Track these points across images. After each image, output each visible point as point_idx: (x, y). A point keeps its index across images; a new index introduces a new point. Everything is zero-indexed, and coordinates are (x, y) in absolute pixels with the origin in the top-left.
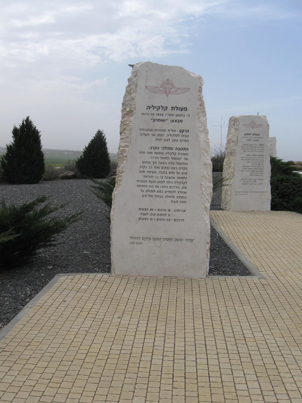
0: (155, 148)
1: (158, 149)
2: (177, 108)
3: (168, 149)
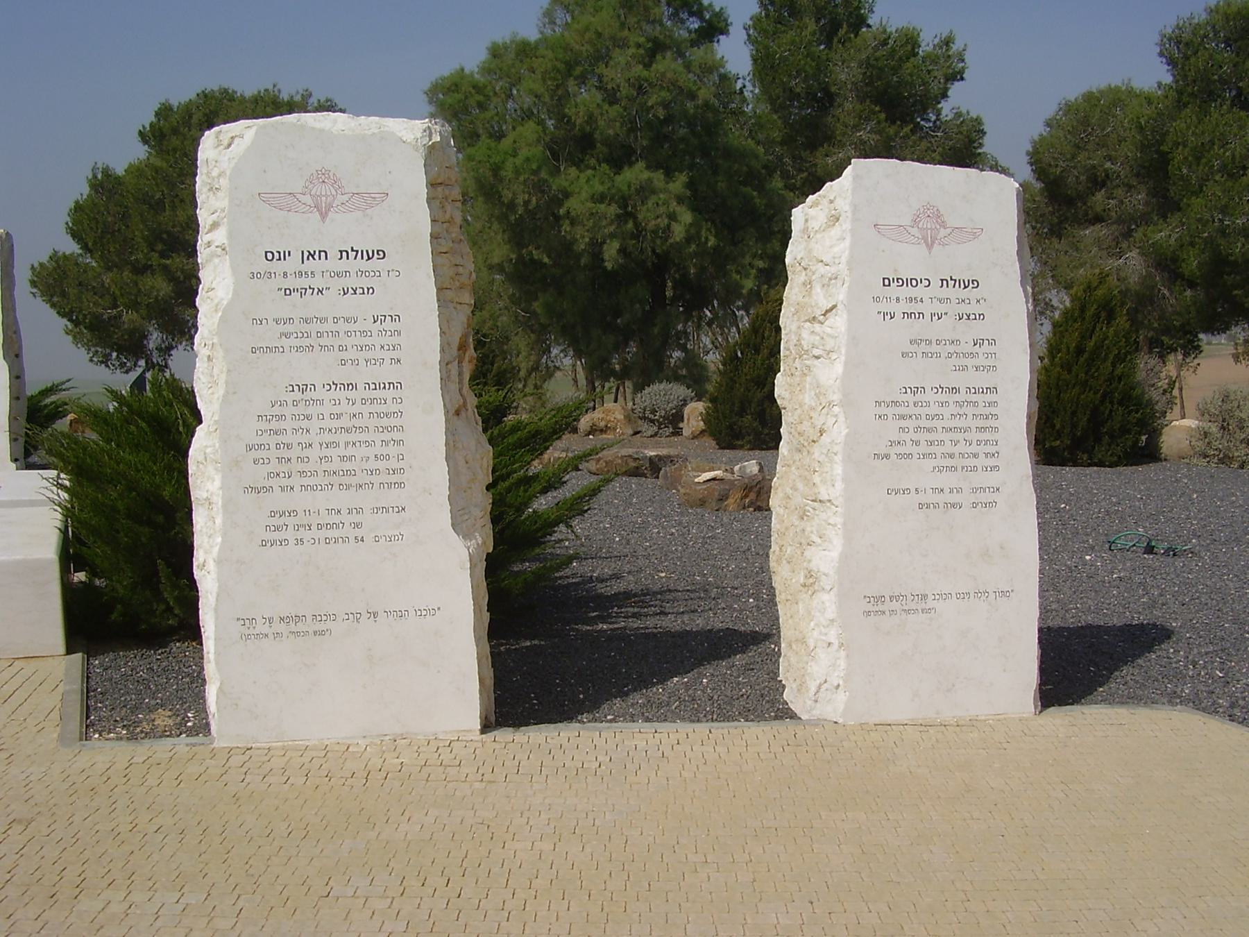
1: (313, 389)
3: (342, 389)
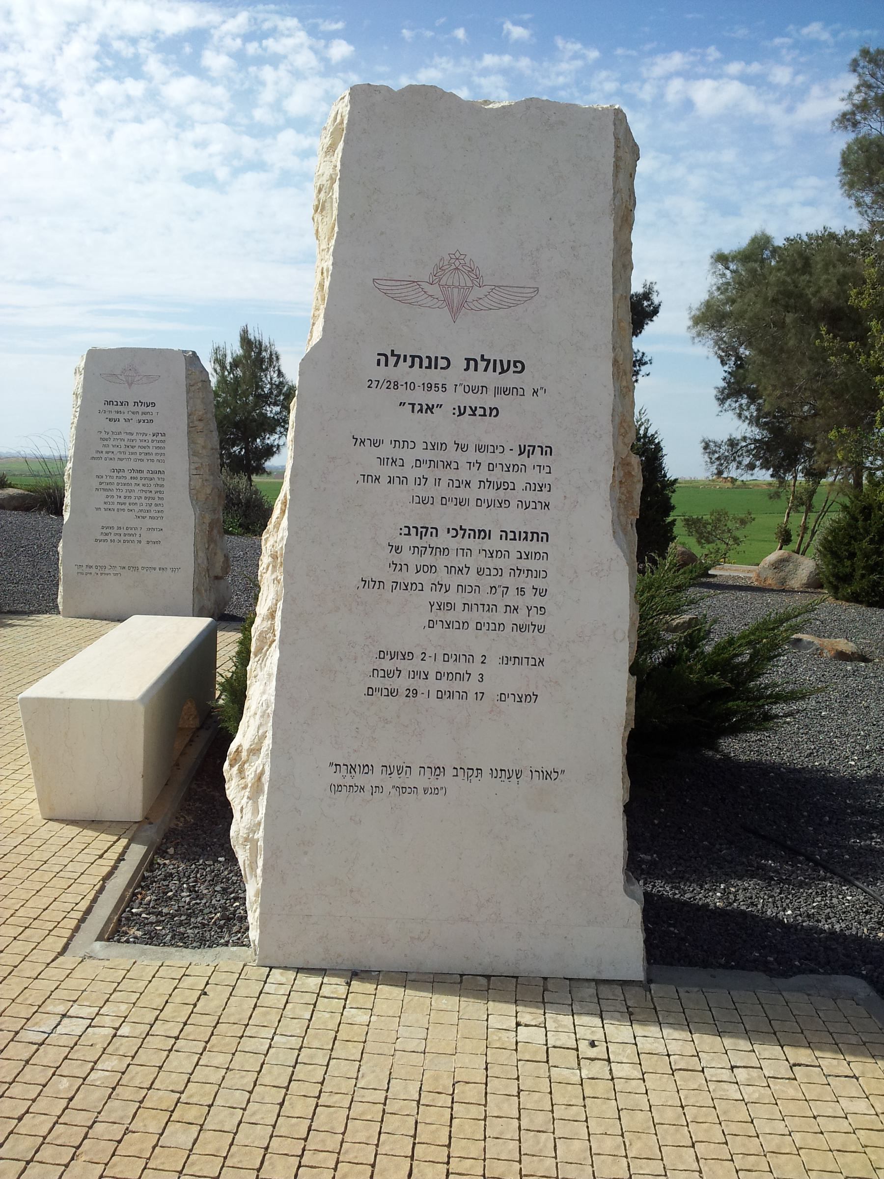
2: (489, 361)
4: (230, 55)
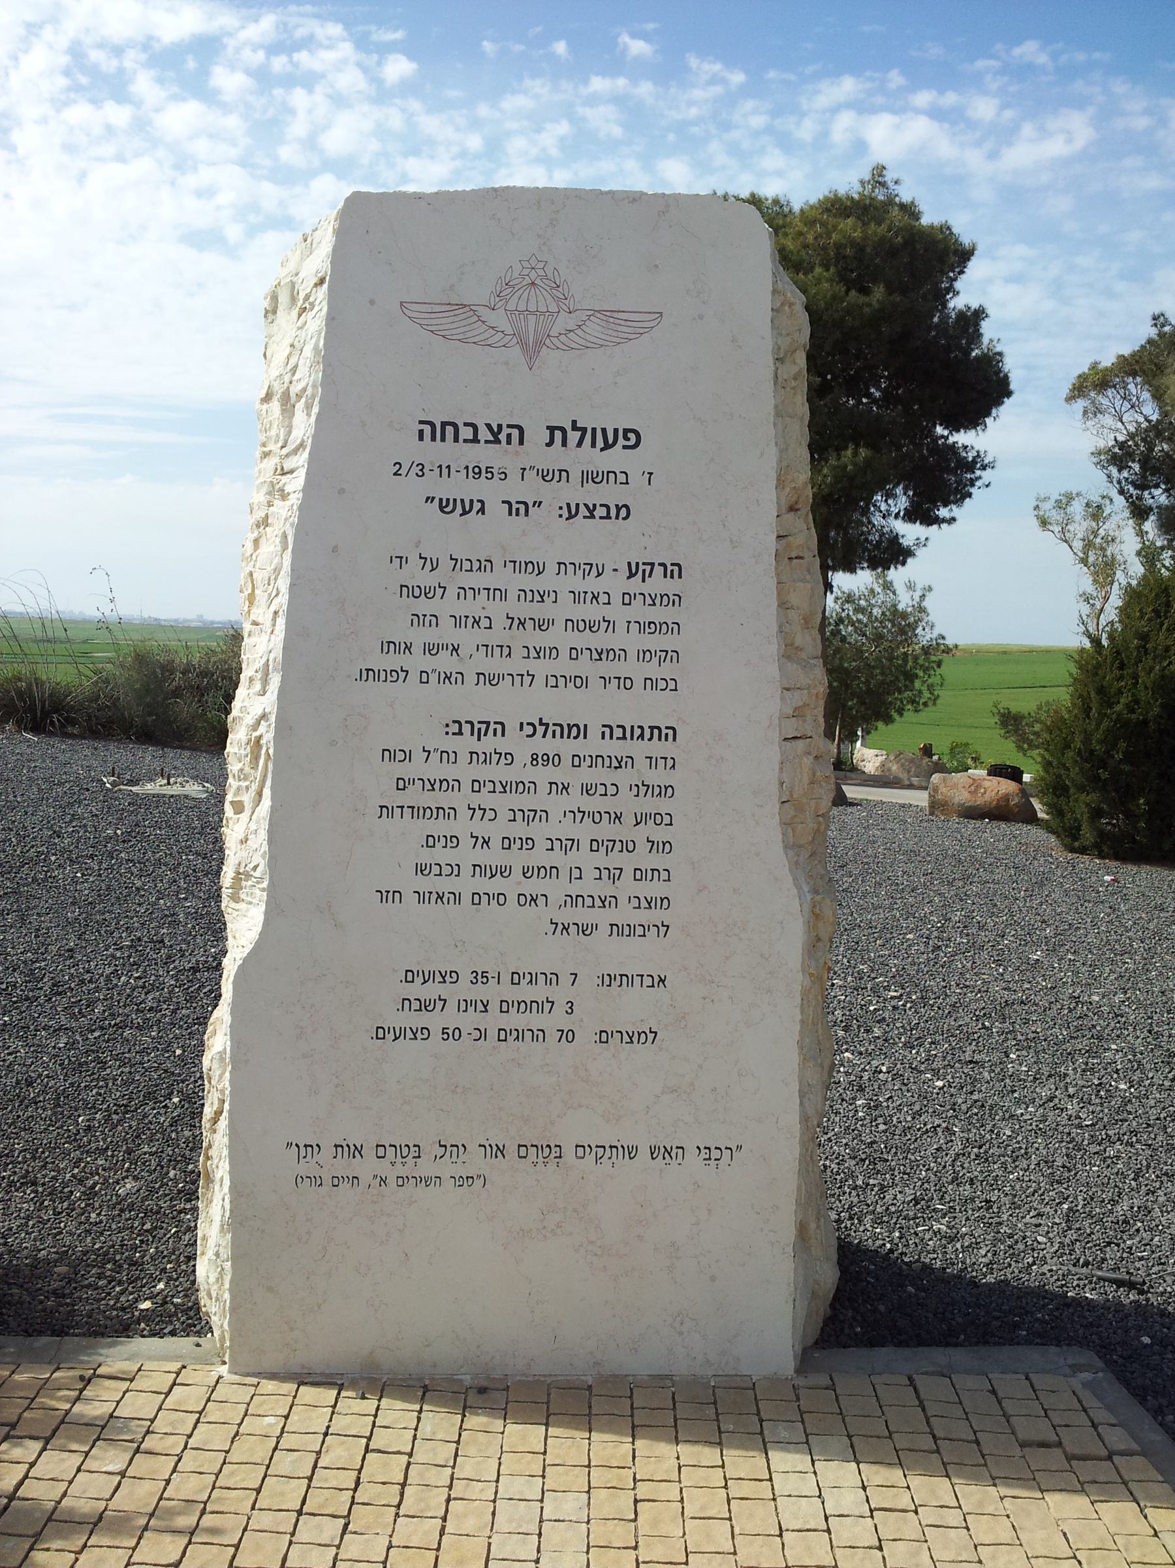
0: (484, 727)
4: (248, 72)
